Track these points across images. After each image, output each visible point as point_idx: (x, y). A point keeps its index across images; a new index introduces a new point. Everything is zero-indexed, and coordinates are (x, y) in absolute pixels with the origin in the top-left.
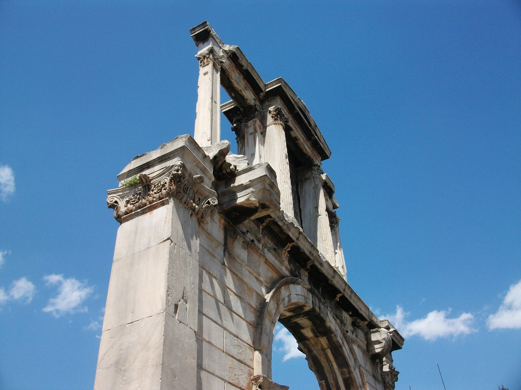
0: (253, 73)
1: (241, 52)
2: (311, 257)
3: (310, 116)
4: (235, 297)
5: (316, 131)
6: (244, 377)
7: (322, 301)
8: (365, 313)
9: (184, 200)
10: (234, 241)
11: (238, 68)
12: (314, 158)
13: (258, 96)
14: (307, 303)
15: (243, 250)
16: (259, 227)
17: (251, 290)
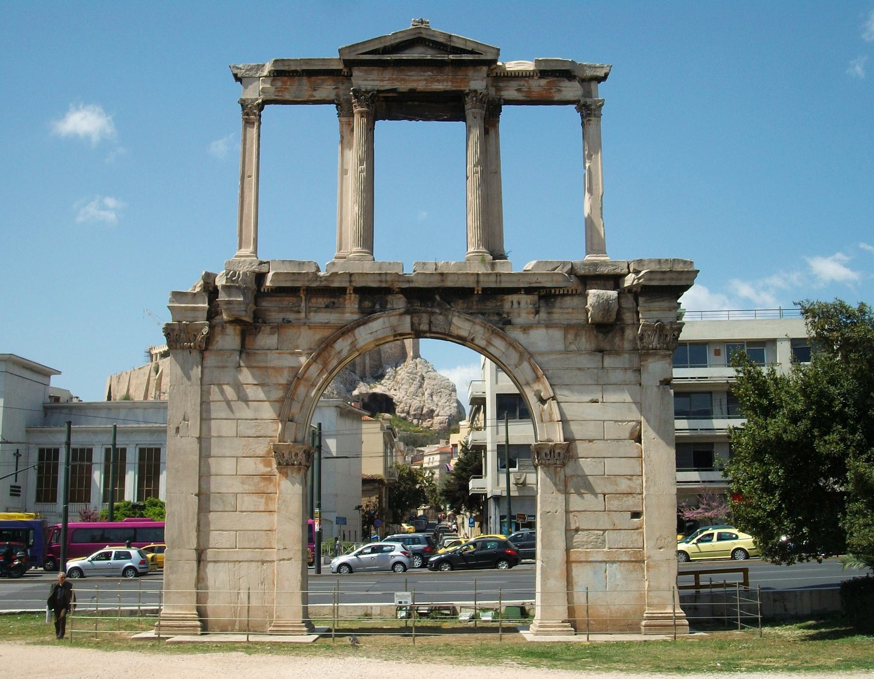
0: (314, 65)
1: (283, 60)
2: (384, 285)
3: (434, 31)
4: (255, 387)
5: (452, 44)
6: (262, 447)
7: (438, 311)
8: (552, 281)
9: (178, 347)
10: (256, 336)
11: (293, 76)
12: (460, 87)
13: (344, 76)
14: (395, 331)
15: (271, 336)
16: (299, 296)
17: (278, 370)
